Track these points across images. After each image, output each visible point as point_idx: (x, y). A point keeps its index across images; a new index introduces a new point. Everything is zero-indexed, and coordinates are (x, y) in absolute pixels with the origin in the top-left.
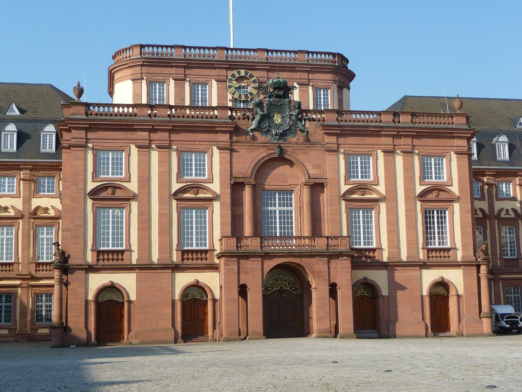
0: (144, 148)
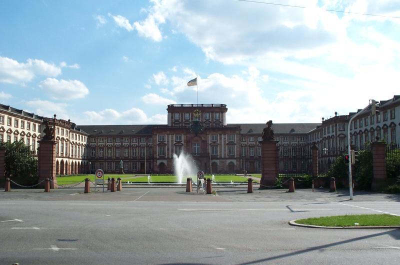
0: (168, 135)
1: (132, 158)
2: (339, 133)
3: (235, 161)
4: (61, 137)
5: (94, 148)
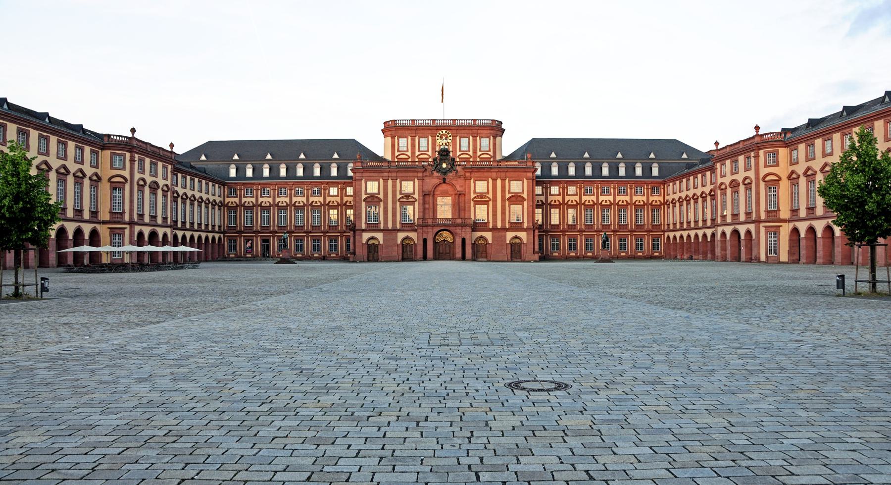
2: (763, 171)
3: (523, 235)
4: (149, 180)
5: (233, 209)
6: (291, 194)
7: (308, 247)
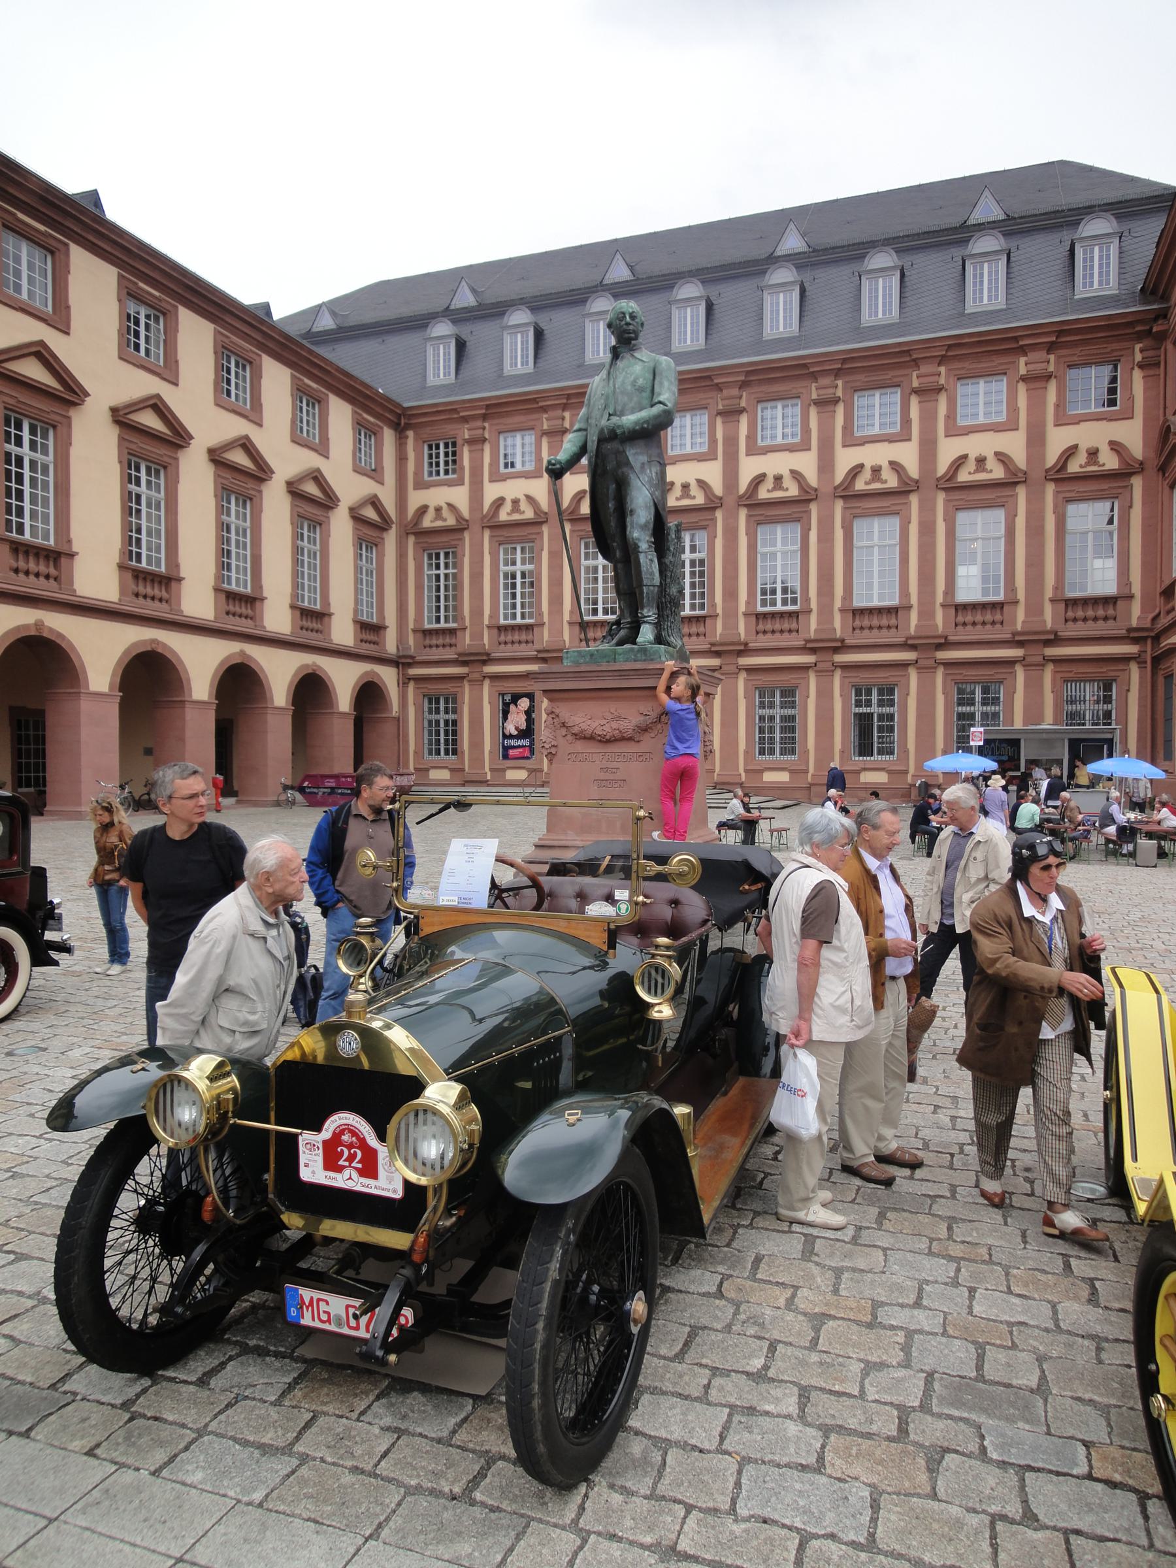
1: (838, 625)
5: (437, 541)
6: (731, 442)
7: (825, 730)
